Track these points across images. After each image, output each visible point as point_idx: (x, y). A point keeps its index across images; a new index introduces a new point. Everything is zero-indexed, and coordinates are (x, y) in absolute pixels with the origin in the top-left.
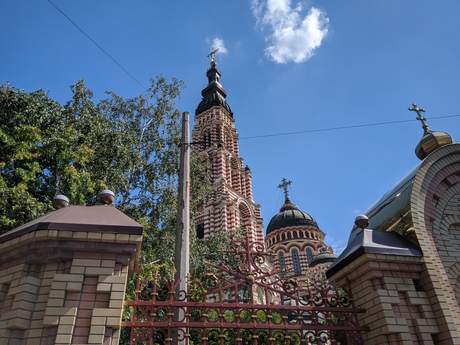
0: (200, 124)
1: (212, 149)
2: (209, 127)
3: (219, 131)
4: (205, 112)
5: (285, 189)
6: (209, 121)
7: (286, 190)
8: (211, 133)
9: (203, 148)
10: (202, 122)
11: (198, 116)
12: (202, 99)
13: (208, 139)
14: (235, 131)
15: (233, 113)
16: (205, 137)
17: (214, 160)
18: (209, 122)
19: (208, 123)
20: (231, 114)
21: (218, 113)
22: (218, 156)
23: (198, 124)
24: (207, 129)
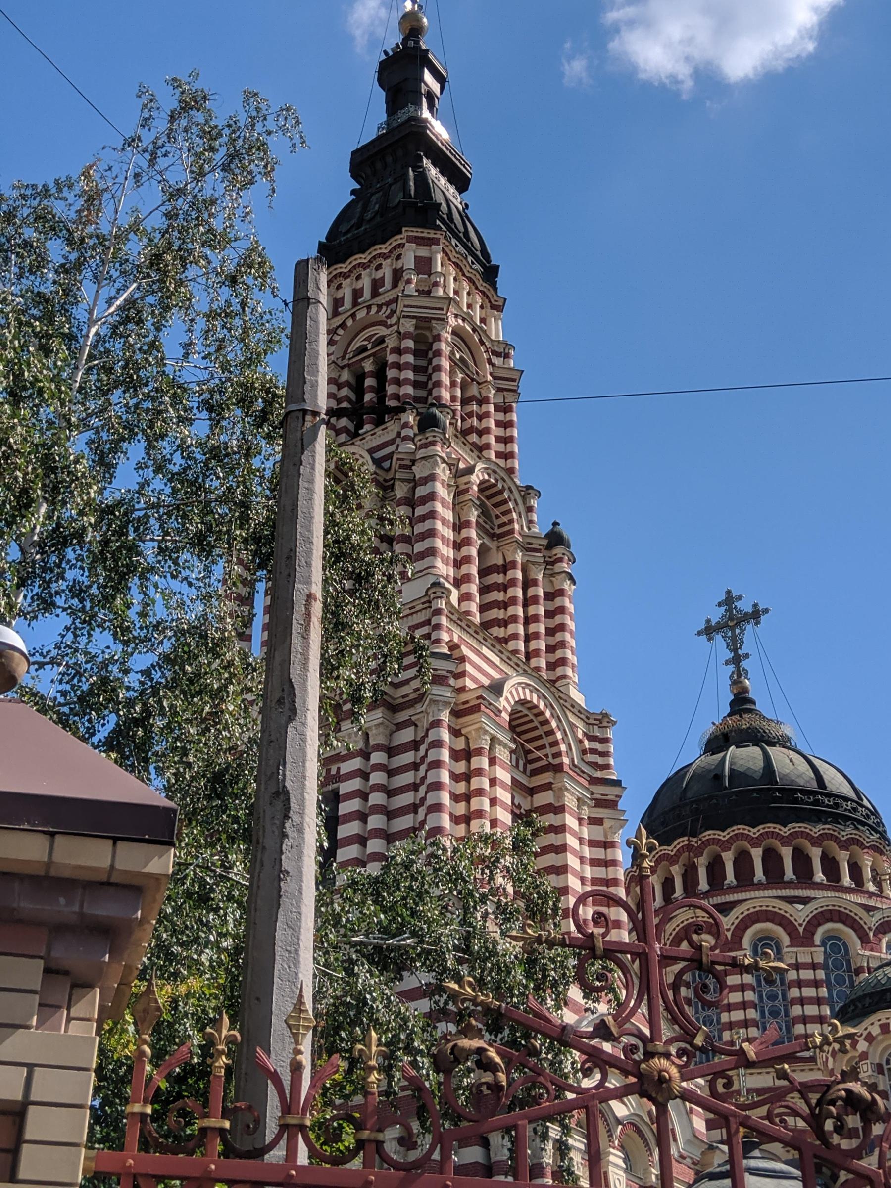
1: (393, 435)
2: (382, 331)
4: (363, 258)
5: (734, 645)
6: (380, 300)
7: (735, 651)
8: (391, 358)
9: (346, 430)
12: (353, 192)
13: (371, 389)
14: (507, 356)
15: (497, 268)
16: (360, 377)
17: (401, 491)
18: (380, 307)
19: (374, 309)
20: (490, 273)
21: (424, 266)
22: (419, 471)
24: (368, 339)
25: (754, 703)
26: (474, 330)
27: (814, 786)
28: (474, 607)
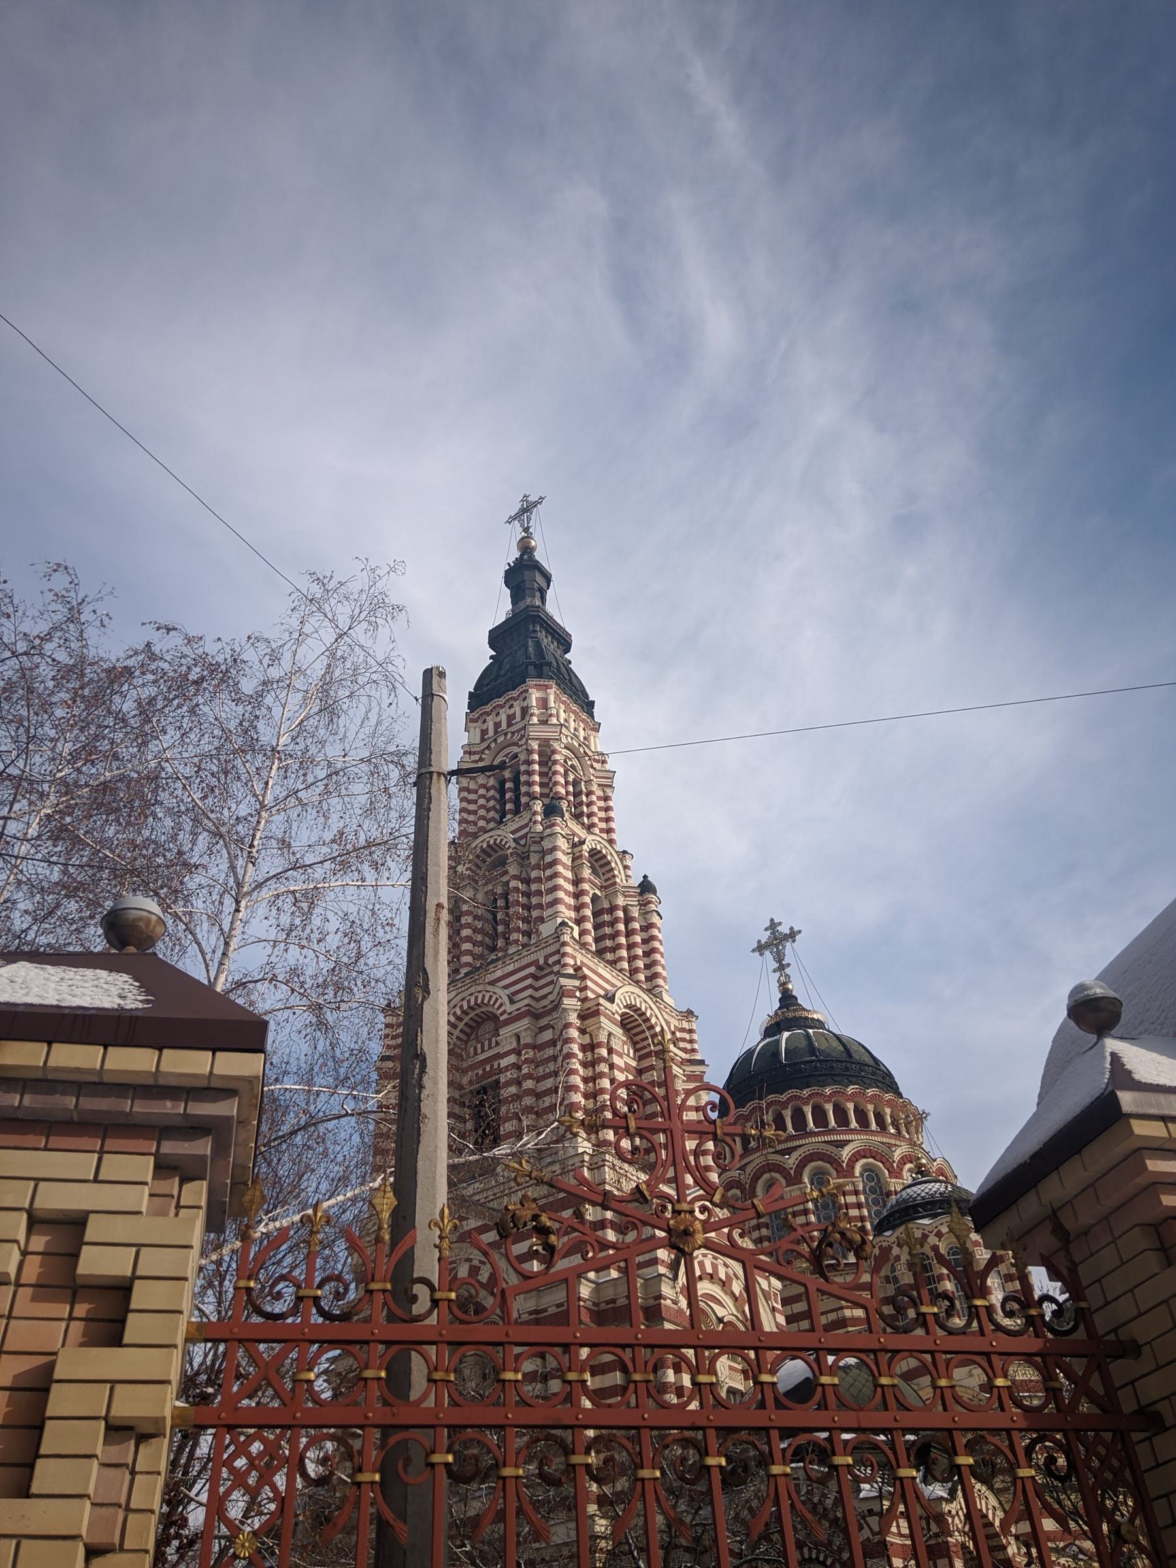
0: (483, 740)
1: (527, 821)
2: (515, 749)
3: (547, 760)
4: (501, 701)
5: (779, 957)
6: (513, 729)
8: (523, 768)
9: (493, 819)
10: (491, 733)
11: (476, 715)
12: (491, 657)
14: (604, 762)
15: (593, 703)
16: (502, 782)
17: (534, 860)
18: (513, 733)
19: (509, 735)
20: (588, 706)
21: (544, 703)
22: (546, 844)
23: (478, 740)
24: (506, 756)
25: (796, 998)
26: (580, 745)
27: (845, 1057)
28: (589, 939)
